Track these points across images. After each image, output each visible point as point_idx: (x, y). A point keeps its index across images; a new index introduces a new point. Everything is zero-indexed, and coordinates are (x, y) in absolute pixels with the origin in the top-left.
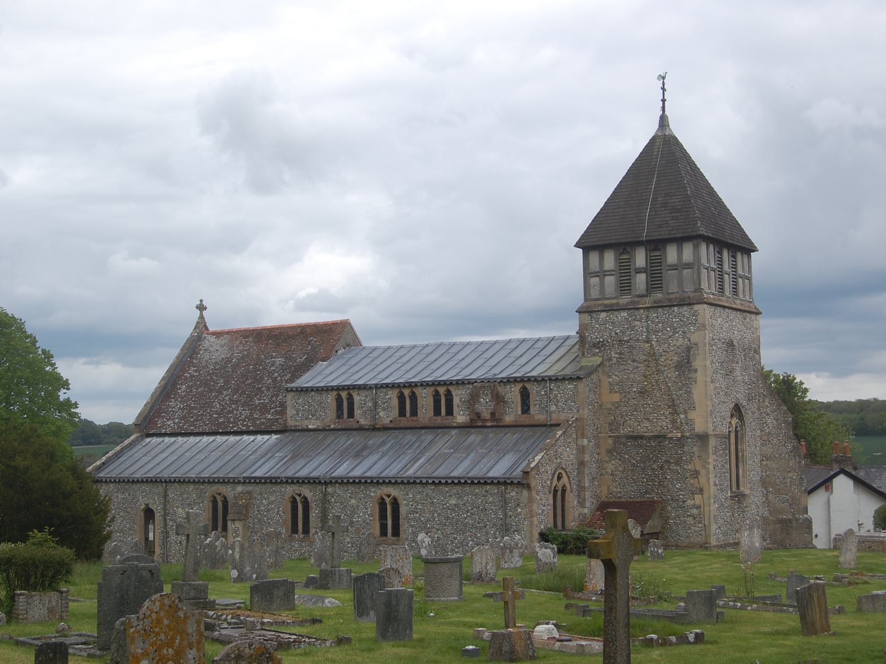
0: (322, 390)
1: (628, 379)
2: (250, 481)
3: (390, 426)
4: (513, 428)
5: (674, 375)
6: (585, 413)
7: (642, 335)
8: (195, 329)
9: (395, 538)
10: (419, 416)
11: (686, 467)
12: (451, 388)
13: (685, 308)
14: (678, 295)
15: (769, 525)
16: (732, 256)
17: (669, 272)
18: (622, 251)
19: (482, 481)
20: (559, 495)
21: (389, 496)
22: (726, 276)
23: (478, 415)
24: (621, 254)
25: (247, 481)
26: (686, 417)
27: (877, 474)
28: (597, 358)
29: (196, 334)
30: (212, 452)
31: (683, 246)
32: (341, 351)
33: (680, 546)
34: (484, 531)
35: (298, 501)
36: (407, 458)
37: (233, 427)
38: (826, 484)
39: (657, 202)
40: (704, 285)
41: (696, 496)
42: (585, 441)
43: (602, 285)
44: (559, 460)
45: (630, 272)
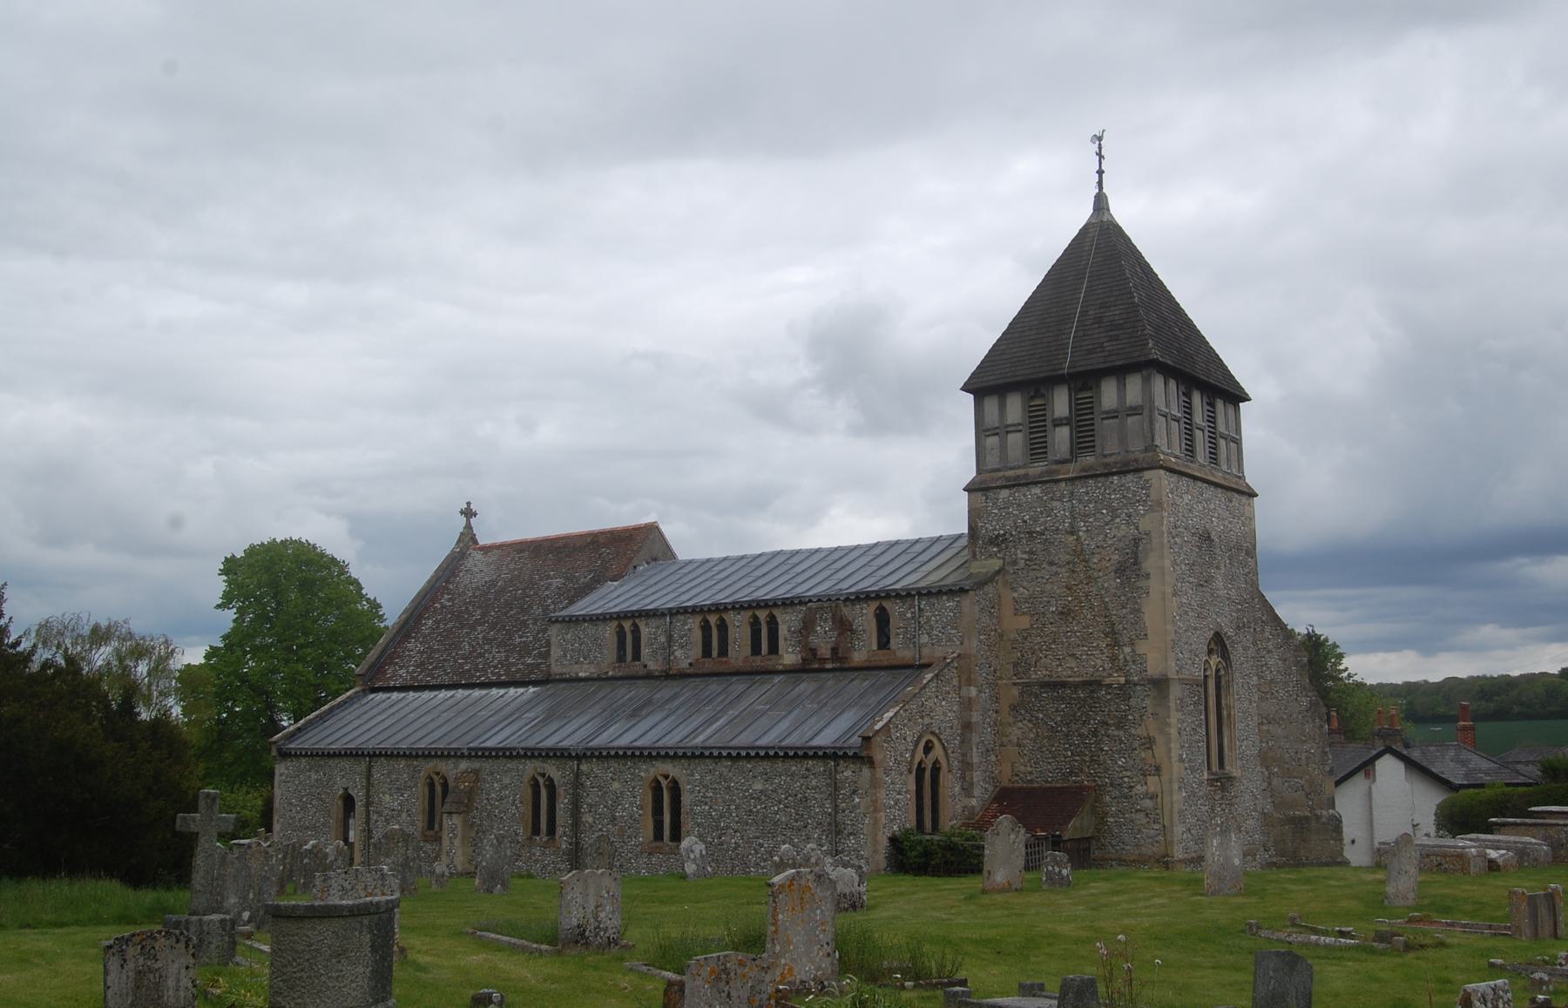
0: (598, 619)
1: (1042, 592)
2: (476, 753)
3: (688, 671)
4: (865, 672)
5: (1114, 585)
6: (973, 645)
7: (1064, 522)
8: (458, 542)
9: (675, 844)
10: (729, 655)
11: (1133, 731)
12: (776, 612)
13: (1130, 477)
14: (1119, 458)
15: (1272, 826)
16: (1208, 404)
17: (1105, 422)
18: (1032, 394)
19: (800, 753)
20: (927, 780)
21: (666, 777)
22: (1198, 433)
23: (813, 651)
24: (1032, 398)
25: (473, 754)
26: (1133, 651)
27: (1439, 754)
28: (995, 560)
29: (458, 550)
30: (443, 712)
31: (1127, 381)
32: (642, 568)
33: (1125, 861)
34: (804, 834)
35: (541, 784)
36: (703, 717)
37: (480, 676)
38: (1366, 767)
39: (1088, 317)
40: (1161, 440)
41: (1150, 779)
42: (973, 691)
43: (1003, 447)
44: (927, 720)
45: (1045, 426)
